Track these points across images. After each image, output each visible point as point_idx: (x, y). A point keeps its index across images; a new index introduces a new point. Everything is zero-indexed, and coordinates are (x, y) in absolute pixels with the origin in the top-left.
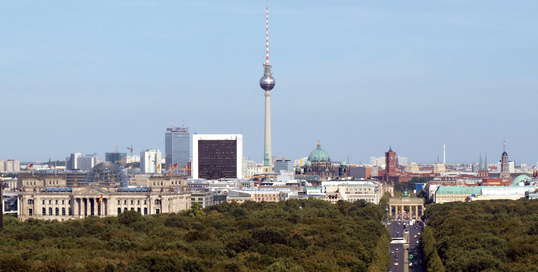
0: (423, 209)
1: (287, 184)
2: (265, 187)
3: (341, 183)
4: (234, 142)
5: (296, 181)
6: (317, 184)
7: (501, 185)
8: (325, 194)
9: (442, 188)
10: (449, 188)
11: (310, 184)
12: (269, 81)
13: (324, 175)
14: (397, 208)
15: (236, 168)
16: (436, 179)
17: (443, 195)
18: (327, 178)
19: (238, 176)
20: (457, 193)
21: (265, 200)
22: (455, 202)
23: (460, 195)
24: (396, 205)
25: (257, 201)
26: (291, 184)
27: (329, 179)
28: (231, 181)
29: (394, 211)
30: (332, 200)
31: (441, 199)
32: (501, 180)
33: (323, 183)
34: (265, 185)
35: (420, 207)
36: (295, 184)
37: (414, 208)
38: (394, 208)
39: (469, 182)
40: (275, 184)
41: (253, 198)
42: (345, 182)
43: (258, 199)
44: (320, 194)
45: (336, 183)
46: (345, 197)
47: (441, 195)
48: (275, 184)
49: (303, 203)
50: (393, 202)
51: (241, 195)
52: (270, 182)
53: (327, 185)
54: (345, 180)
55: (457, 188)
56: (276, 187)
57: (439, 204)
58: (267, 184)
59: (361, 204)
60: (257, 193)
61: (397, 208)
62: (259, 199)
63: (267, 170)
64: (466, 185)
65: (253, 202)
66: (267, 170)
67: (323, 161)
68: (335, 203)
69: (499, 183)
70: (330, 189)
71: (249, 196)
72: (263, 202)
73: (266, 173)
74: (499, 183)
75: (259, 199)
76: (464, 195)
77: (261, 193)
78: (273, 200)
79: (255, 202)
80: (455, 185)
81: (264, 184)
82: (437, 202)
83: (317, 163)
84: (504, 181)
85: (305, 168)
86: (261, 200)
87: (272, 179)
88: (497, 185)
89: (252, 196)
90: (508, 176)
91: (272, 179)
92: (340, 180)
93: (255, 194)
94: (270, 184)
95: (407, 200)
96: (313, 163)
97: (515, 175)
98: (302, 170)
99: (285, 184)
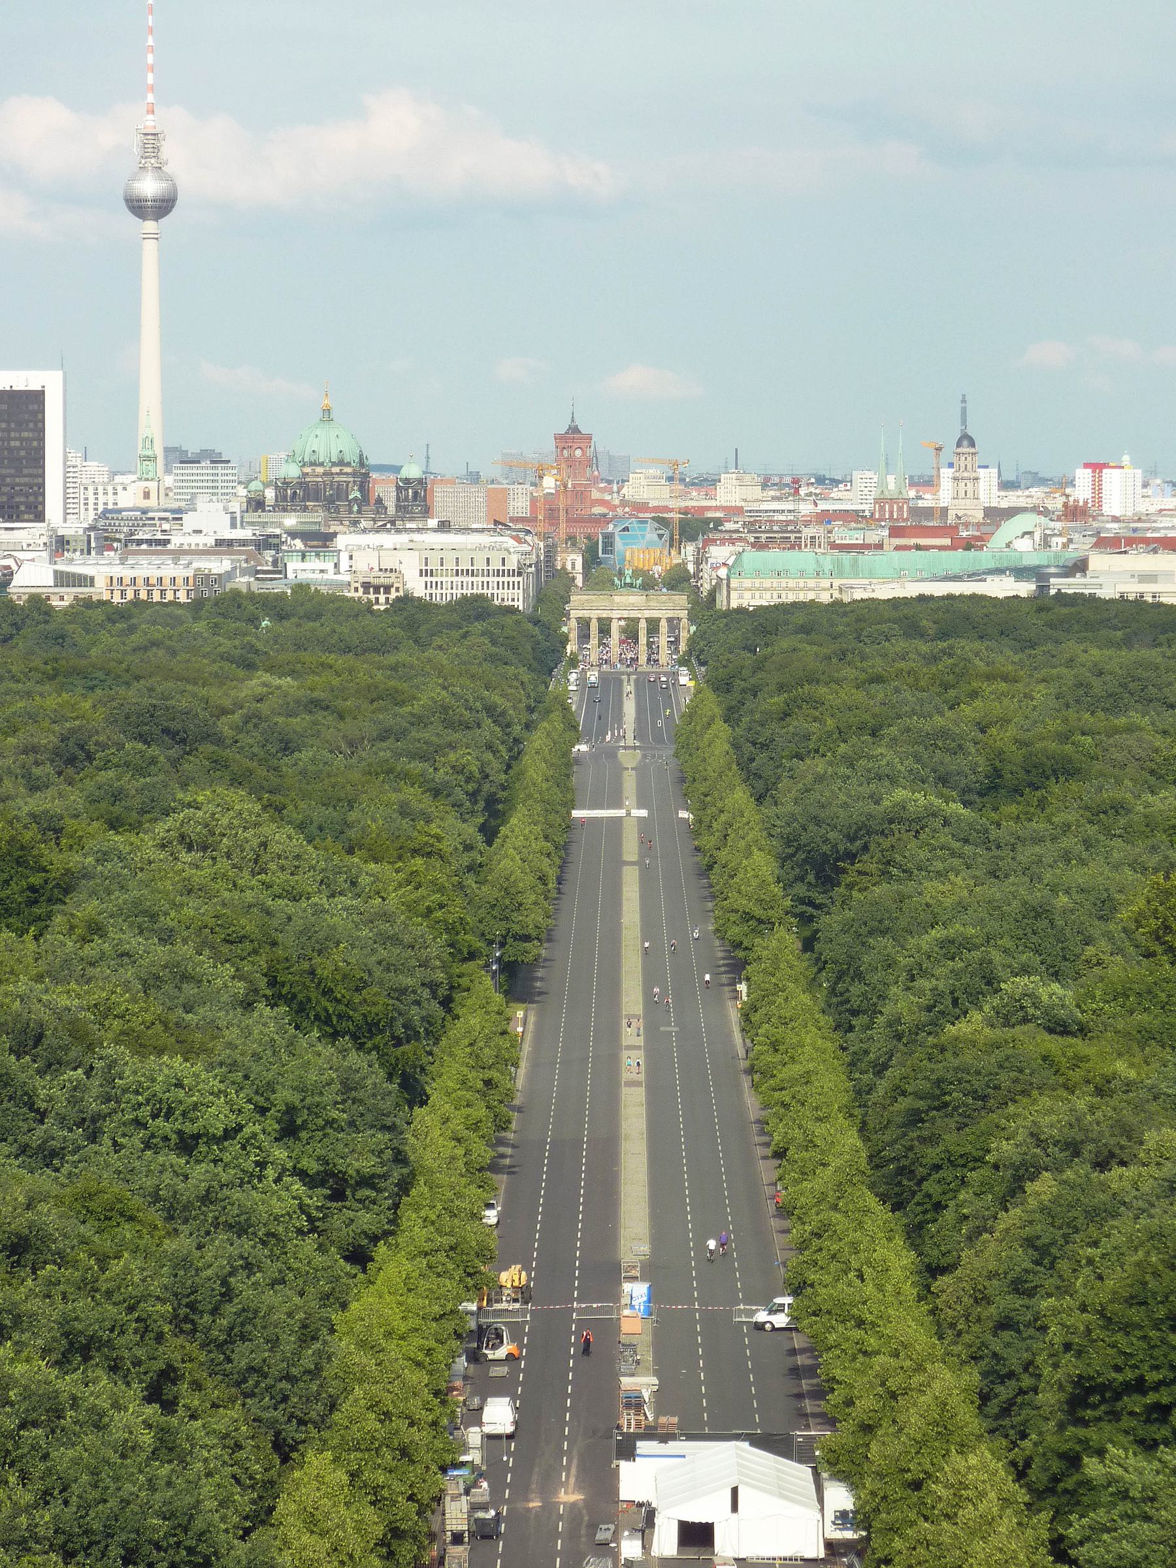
0: (687, 630)
1: (219, 543)
2: (145, 552)
3: (404, 538)
4: (37, 398)
5: (246, 533)
6: (319, 541)
7: (952, 548)
8: (346, 578)
9: (752, 558)
10: (775, 557)
11: (298, 544)
12: (149, 187)
13: (343, 514)
14: (594, 626)
15: (42, 486)
16: (729, 526)
17: (756, 583)
18: (355, 523)
19: (47, 517)
20: (802, 574)
21: (143, 596)
22: (794, 604)
23: (811, 583)
24: (594, 615)
25: (117, 599)
26: (230, 543)
27: (364, 524)
28: (28, 533)
29: (584, 637)
30: (372, 597)
31: (747, 595)
32: (955, 528)
33: (341, 541)
34: (144, 547)
35: (673, 623)
36: (243, 543)
37: (653, 626)
38: (584, 624)
39: (845, 534)
40: (176, 541)
41: (100, 591)
42: (416, 537)
43: (117, 595)
44: (330, 576)
45: (388, 540)
46: (418, 588)
47: (747, 583)
48: (176, 541)
49: (277, 607)
50: (583, 606)
51: (62, 579)
52: (159, 536)
53: (359, 547)
54: (419, 530)
55: (802, 559)
56: (178, 554)
57: (741, 611)
58: (149, 542)
59: (475, 608)
60: (118, 571)
61: (594, 626)
62: (123, 593)
63: (147, 495)
64: (834, 546)
65: (101, 603)
66: (147, 495)
67: (341, 463)
68: (382, 608)
69: (947, 541)
70: (365, 559)
71: (90, 581)
72: (137, 603)
73: (145, 504)
74: (947, 541)
75: (123, 593)
76: (826, 583)
77: (127, 573)
78: (169, 596)
79: (108, 603)
80: (795, 546)
81: (139, 542)
82: (734, 604)
83: (320, 470)
84: (964, 534)
85: (282, 487)
86: (130, 595)
87: (166, 526)
88: (941, 548)
89: (101, 584)
90: (979, 516)
91: (166, 526)
92: (398, 531)
93: (106, 575)
94: (159, 542)
95: (633, 599)
96: (308, 470)
97: (996, 516)
98: (270, 494)
99: (211, 541)
